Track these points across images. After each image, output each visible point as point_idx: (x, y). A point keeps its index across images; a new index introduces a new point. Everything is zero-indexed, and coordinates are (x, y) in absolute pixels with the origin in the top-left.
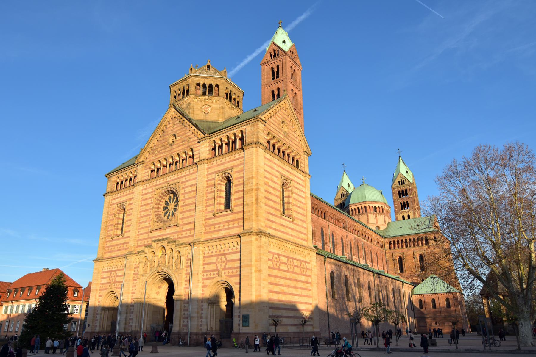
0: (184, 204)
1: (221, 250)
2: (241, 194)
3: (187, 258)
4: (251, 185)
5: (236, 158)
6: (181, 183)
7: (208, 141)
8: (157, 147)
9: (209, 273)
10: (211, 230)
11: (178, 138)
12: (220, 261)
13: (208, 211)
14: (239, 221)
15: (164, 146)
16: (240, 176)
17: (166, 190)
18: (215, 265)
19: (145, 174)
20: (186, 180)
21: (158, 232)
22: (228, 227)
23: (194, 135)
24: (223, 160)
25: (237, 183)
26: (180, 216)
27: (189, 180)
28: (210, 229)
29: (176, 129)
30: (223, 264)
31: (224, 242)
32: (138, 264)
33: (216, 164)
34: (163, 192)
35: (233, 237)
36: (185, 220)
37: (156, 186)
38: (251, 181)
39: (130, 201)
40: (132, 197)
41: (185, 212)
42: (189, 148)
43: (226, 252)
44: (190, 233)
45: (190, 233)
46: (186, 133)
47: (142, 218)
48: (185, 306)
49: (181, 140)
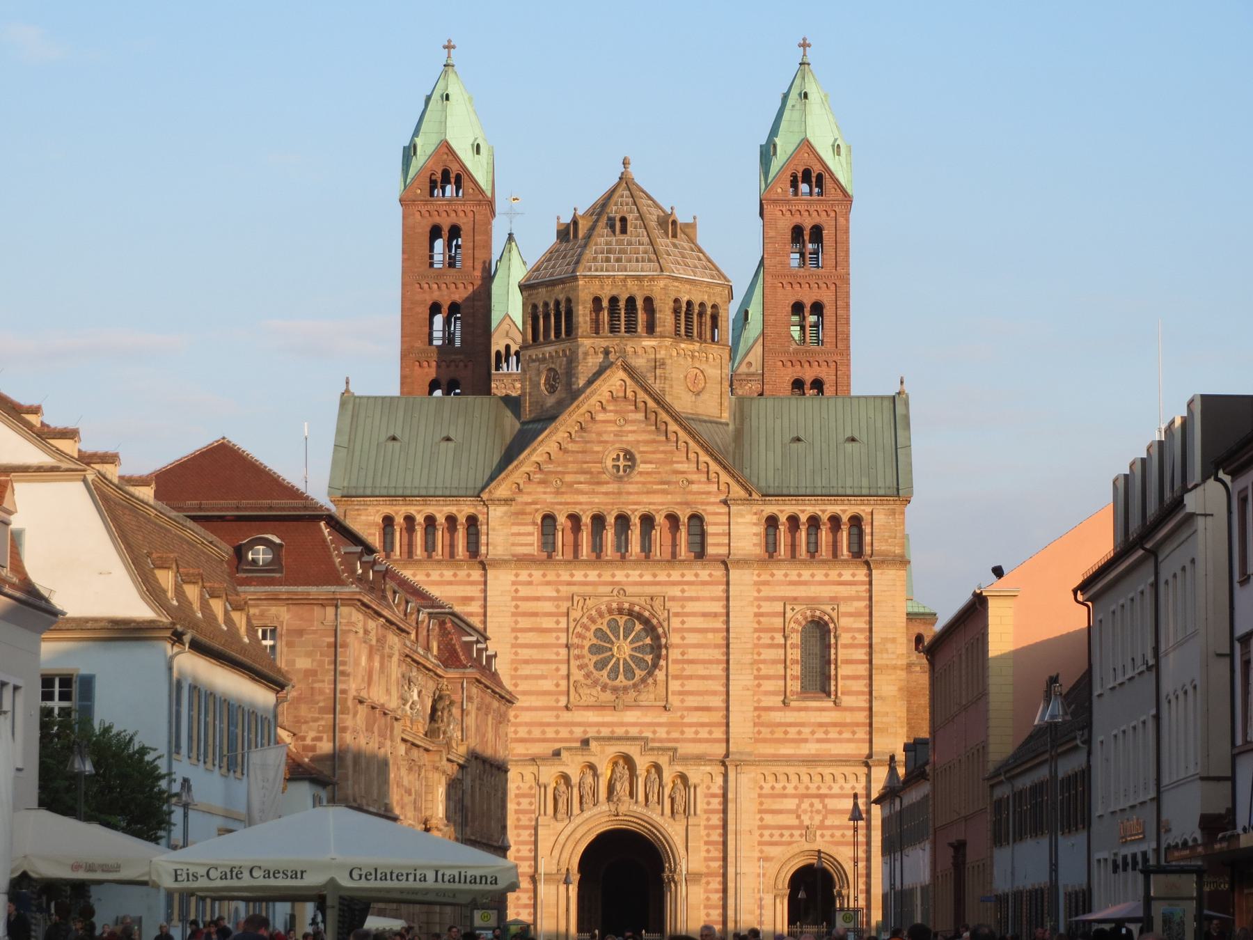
0: (685, 657)
1: (810, 785)
2: (862, 670)
3: (706, 791)
4: (894, 656)
5: (843, 578)
6: (669, 600)
7: (755, 508)
8: (560, 469)
9: (777, 833)
10: (776, 736)
11: (642, 466)
12: (809, 809)
13: (763, 688)
14: (855, 729)
15: (591, 473)
16: (856, 625)
17: (614, 605)
18: (795, 816)
19: (518, 538)
20: (686, 594)
21: (600, 712)
22: (824, 736)
23: (703, 478)
24: (806, 574)
25: (850, 641)
26: (674, 685)
27: (697, 599)
28: (772, 733)
29: (631, 438)
30: (818, 819)
31: (820, 769)
32: (531, 788)
33: (783, 578)
34: (603, 608)
35: (848, 763)
36: (691, 698)
37: (569, 584)
38: (890, 646)
39: (464, 605)
40: (469, 595)
41: (690, 677)
42: (689, 512)
43: (824, 791)
44: (710, 733)
45: (710, 733)
46: (673, 462)
47: (523, 666)
48: (708, 899)
49: (656, 478)
